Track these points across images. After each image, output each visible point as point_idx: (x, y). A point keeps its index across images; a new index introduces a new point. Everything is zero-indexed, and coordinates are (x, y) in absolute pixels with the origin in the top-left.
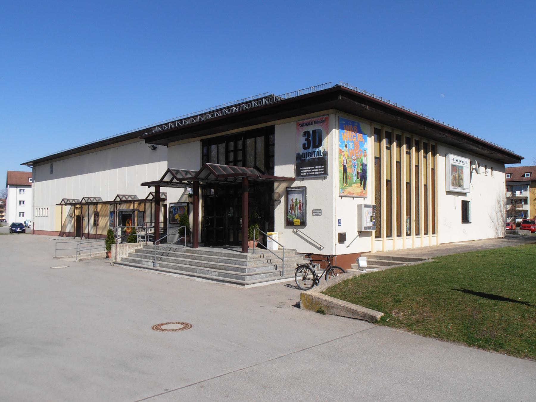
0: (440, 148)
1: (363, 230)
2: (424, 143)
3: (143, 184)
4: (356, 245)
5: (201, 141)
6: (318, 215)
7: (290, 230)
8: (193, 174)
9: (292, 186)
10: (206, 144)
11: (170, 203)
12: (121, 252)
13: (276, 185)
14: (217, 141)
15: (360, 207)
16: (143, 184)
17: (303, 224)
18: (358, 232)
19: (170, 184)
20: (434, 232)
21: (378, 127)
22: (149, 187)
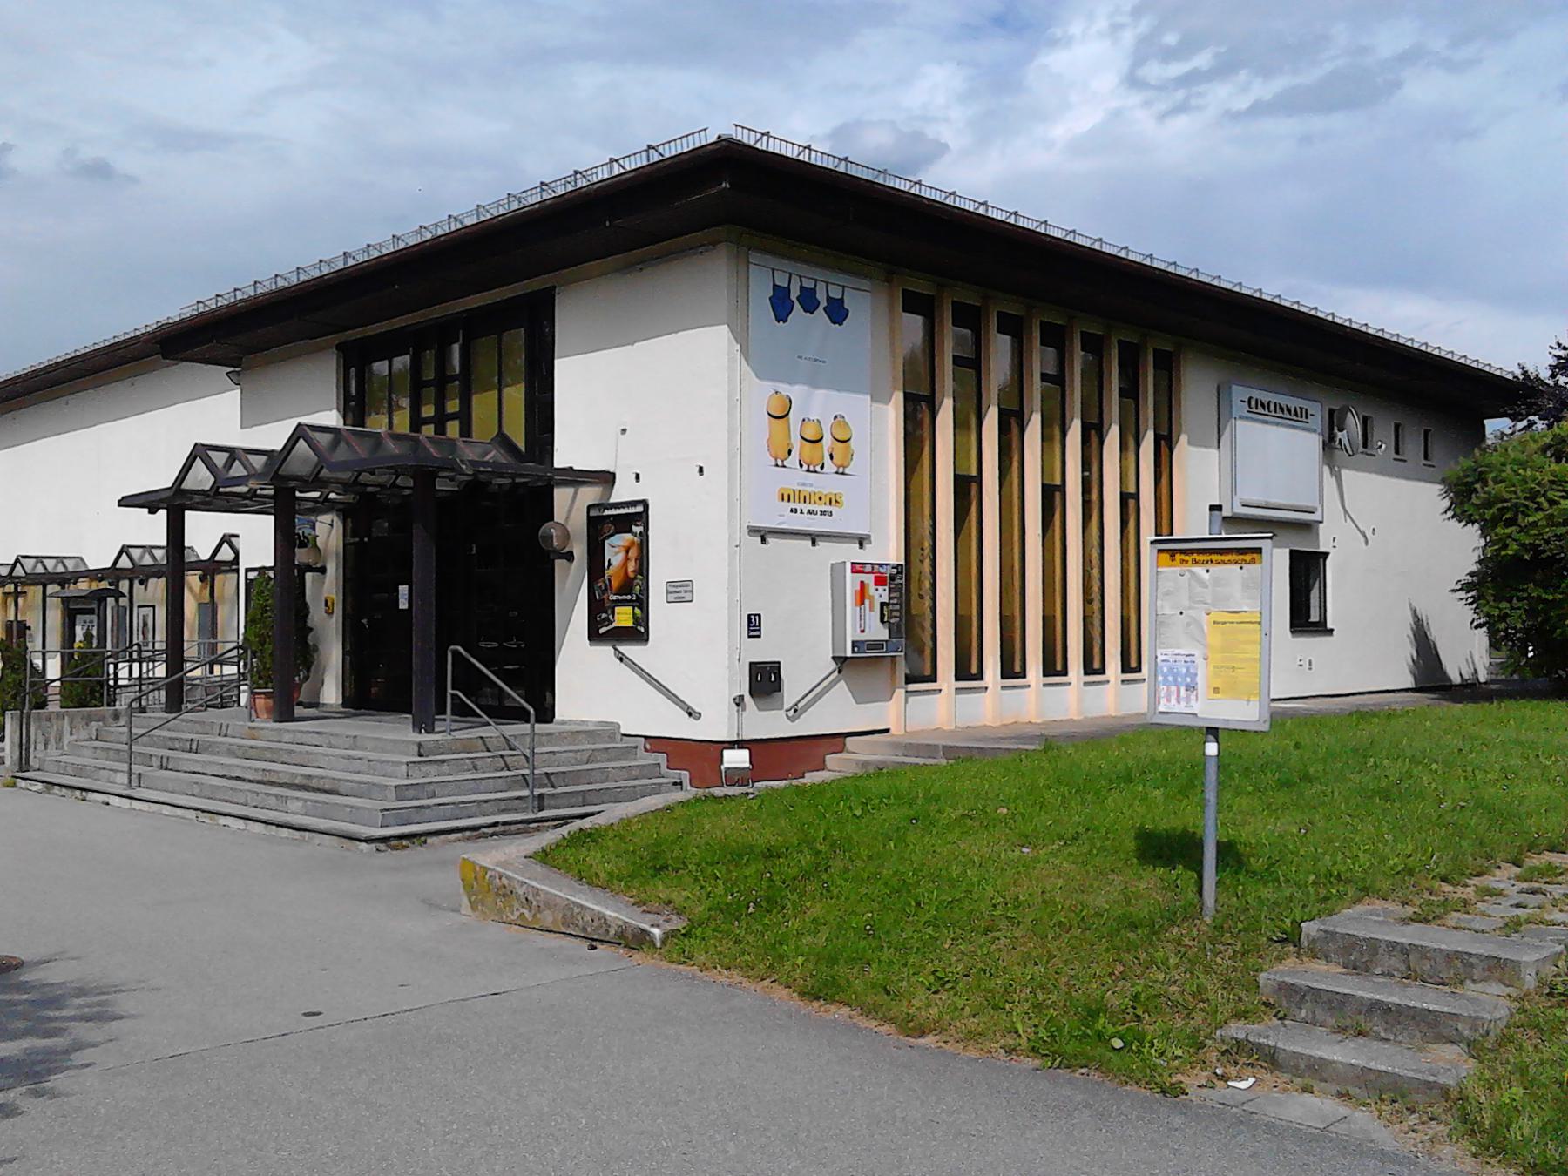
0: (1197, 391)
1: (849, 654)
2: (1045, 327)
3: (126, 502)
4: (837, 711)
5: (338, 347)
6: (681, 600)
7: (606, 651)
8: (258, 462)
9: (612, 500)
10: (355, 360)
11: (247, 570)
12: (41, 739)
13: (561, 496)
14: (387, 347)
15: (836, 569)
16: (126, 502)
17: (638, 634)
18: (834, 658)
19: (212, 501)
20: (1130, 665)
21: (922, 287)
22: (153, 511)
